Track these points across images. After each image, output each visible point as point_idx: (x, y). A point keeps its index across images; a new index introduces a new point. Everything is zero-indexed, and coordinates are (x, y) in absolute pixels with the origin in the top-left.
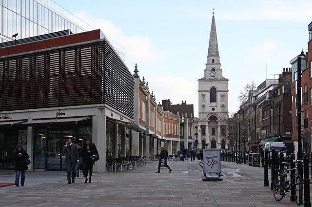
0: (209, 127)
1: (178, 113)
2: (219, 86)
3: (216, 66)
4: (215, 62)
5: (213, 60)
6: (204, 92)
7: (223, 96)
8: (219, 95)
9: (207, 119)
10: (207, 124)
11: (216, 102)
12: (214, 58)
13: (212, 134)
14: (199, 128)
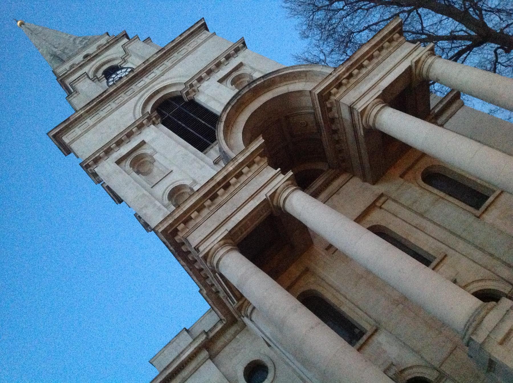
6: (119, 143)
10: (267, 181)
12: (85, 53)
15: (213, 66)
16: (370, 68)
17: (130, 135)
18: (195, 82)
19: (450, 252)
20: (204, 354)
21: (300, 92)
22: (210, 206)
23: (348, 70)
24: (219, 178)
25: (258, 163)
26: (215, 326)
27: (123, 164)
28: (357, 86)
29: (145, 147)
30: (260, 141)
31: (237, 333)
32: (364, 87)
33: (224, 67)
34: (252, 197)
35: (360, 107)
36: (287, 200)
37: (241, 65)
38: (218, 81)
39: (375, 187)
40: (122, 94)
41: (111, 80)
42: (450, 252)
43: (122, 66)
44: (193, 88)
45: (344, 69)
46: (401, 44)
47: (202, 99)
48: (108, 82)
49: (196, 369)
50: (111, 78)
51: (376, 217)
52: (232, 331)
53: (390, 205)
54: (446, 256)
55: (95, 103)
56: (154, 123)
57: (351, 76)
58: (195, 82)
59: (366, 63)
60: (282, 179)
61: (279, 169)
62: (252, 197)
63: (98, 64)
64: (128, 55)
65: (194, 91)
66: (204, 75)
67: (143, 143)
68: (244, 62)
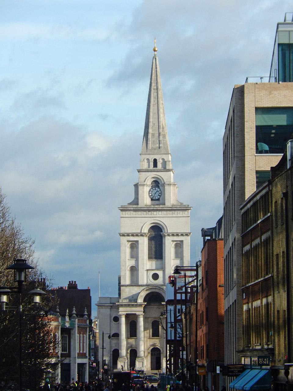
0: (145, 319)
1: (58, 310)
5: (155, 161)
6: (133, 235)
9: (140, 300)
10: (139, 311)
11: (162, 259)
13: (153, 336)
14: (123, 320)
15: (175, 234)
18: (166, 234)
60: (142, 313)
67: (138, 241)
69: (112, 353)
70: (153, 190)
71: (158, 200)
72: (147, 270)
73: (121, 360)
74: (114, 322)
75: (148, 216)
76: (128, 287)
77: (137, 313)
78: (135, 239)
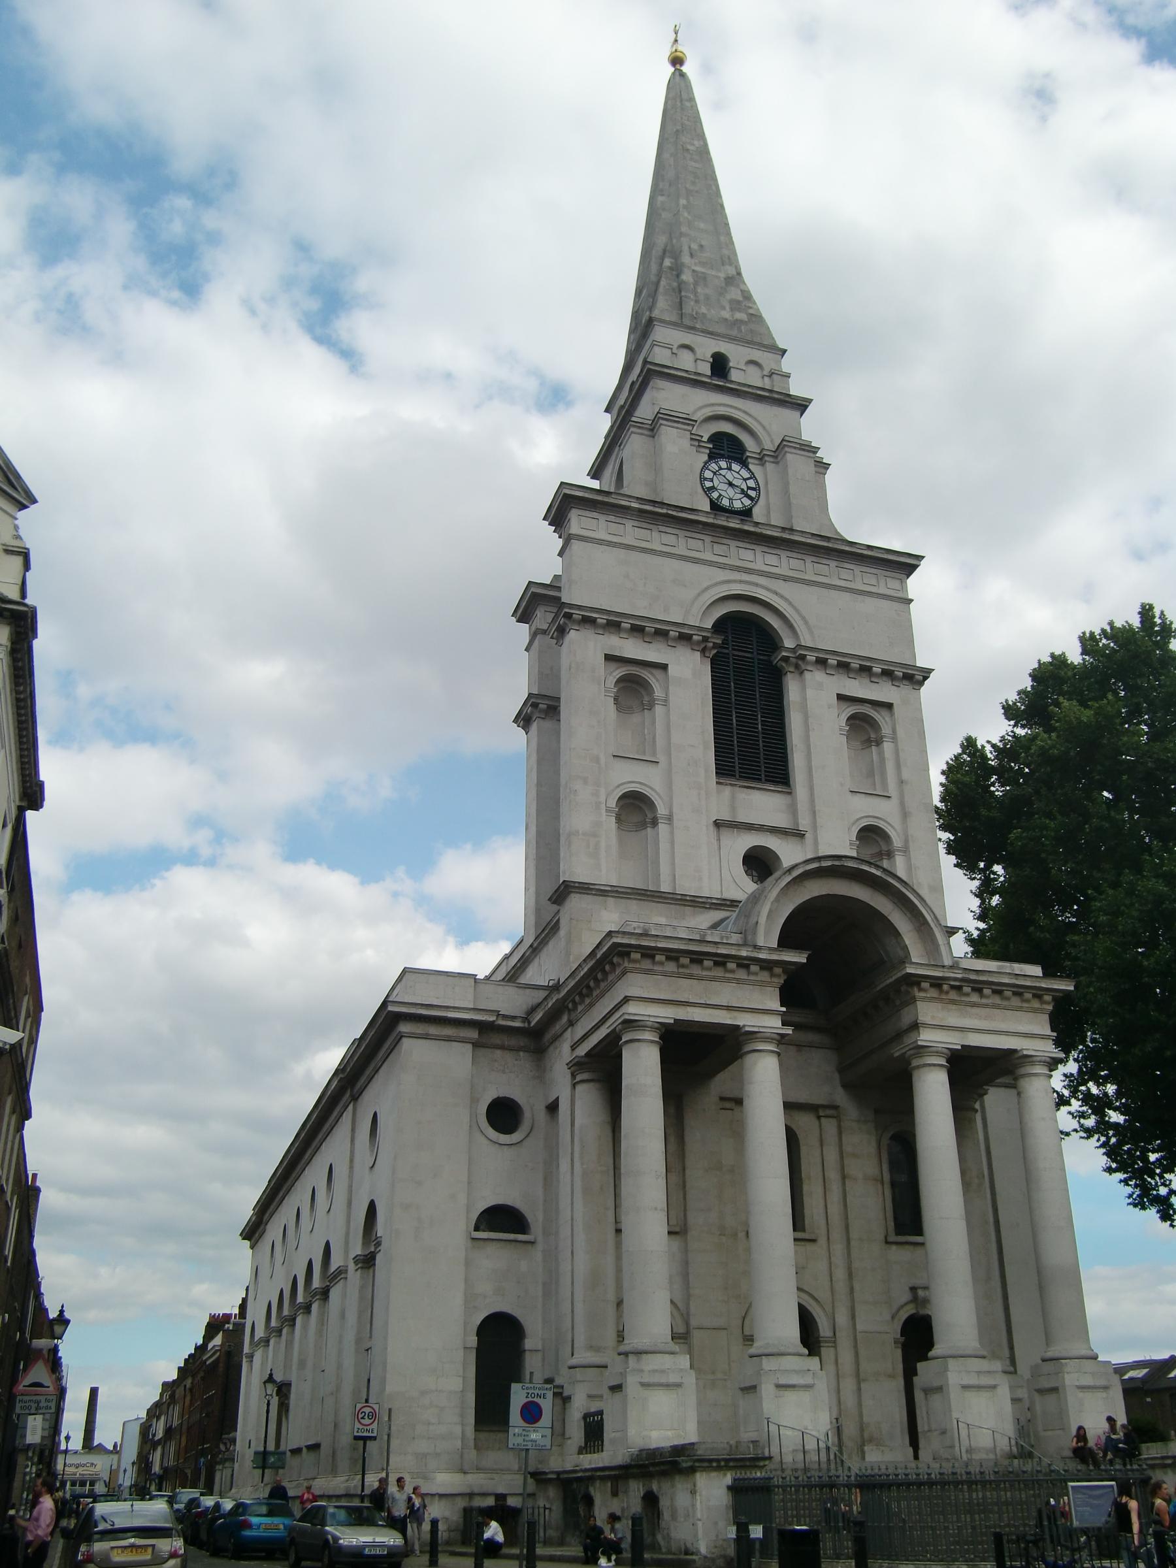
2: (814, 612)
3: (768, 423)
4: (735, 375)
5: (720, 365)
6: (637, 630)
7: (864, 725)
8: (813, 711)
10: (758, 1009)
12: (724, 347)
15: (855, 664)
16: (984, 1001)
17: (661, 634)
18: (811, 657)
19: (822, 1241)
20: (473, 1034)
21: (897, 934)
22: (683, 966)
23: (962, 980)
24: (723, 950)
25: (772, 975)
26: (513, 1018)
27: (613, 665)
28: (950, 1006)
29: (658, 673)
30: (798, 958)
31: (525, 1049)
32: (953, 1019)
33: (867, 681)
34: (729, 1008)
35: (926, 1037)
36: (756, 1054)
37: (889, 706)
38: (838, 695)
39: (840, 1090)
40: (708, 539)
41: (714, 466)
42: (822, 1241)
43: (750, 460)
44: (800, 662)
45: (959, 976)
46: (1041, 1011)
47: (792, 688)
48: (705, 467)
49: (449, 1039)
50: (716, 463)
51: (805, 1122)
52: (522, 1041)
53: (830, 1126)
54: (813, 1241)
55: (664, 511)
56: (703, 651)
57: (959, 988)
58: (811, 657)
59: (987, 991)
60: (773, 1024)
61: (784, 1009)
62: (729, 1008)
63: (722, 411)
64: (776, 457)
65: (797, 666)
66: (832, 662)
67: (664, 667)
68: (895, 707)
69: (473, 1340)
70: (721, 469)
71: (746, 513)
72: (718, 824)
73: (655, 1371)
74: (492, 1133)
75: (708, 556)
76: (611, 901)
77: (747, 1021)
78: (652, 653)
